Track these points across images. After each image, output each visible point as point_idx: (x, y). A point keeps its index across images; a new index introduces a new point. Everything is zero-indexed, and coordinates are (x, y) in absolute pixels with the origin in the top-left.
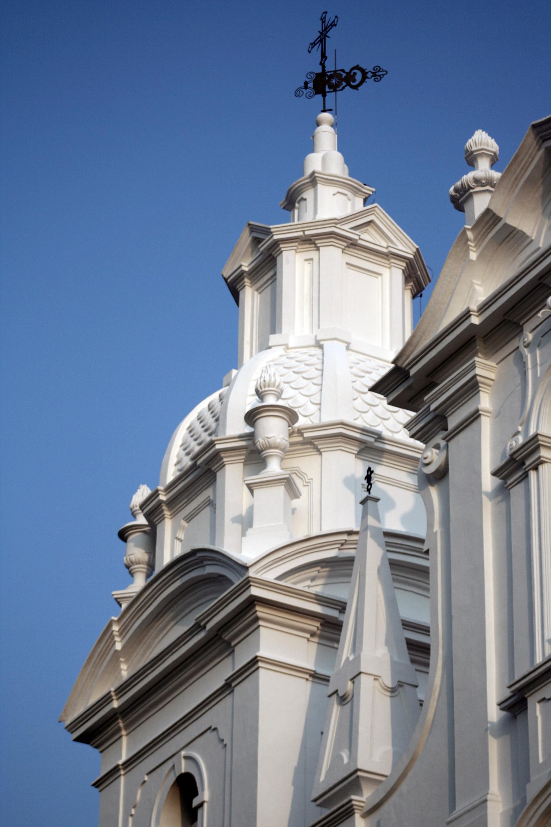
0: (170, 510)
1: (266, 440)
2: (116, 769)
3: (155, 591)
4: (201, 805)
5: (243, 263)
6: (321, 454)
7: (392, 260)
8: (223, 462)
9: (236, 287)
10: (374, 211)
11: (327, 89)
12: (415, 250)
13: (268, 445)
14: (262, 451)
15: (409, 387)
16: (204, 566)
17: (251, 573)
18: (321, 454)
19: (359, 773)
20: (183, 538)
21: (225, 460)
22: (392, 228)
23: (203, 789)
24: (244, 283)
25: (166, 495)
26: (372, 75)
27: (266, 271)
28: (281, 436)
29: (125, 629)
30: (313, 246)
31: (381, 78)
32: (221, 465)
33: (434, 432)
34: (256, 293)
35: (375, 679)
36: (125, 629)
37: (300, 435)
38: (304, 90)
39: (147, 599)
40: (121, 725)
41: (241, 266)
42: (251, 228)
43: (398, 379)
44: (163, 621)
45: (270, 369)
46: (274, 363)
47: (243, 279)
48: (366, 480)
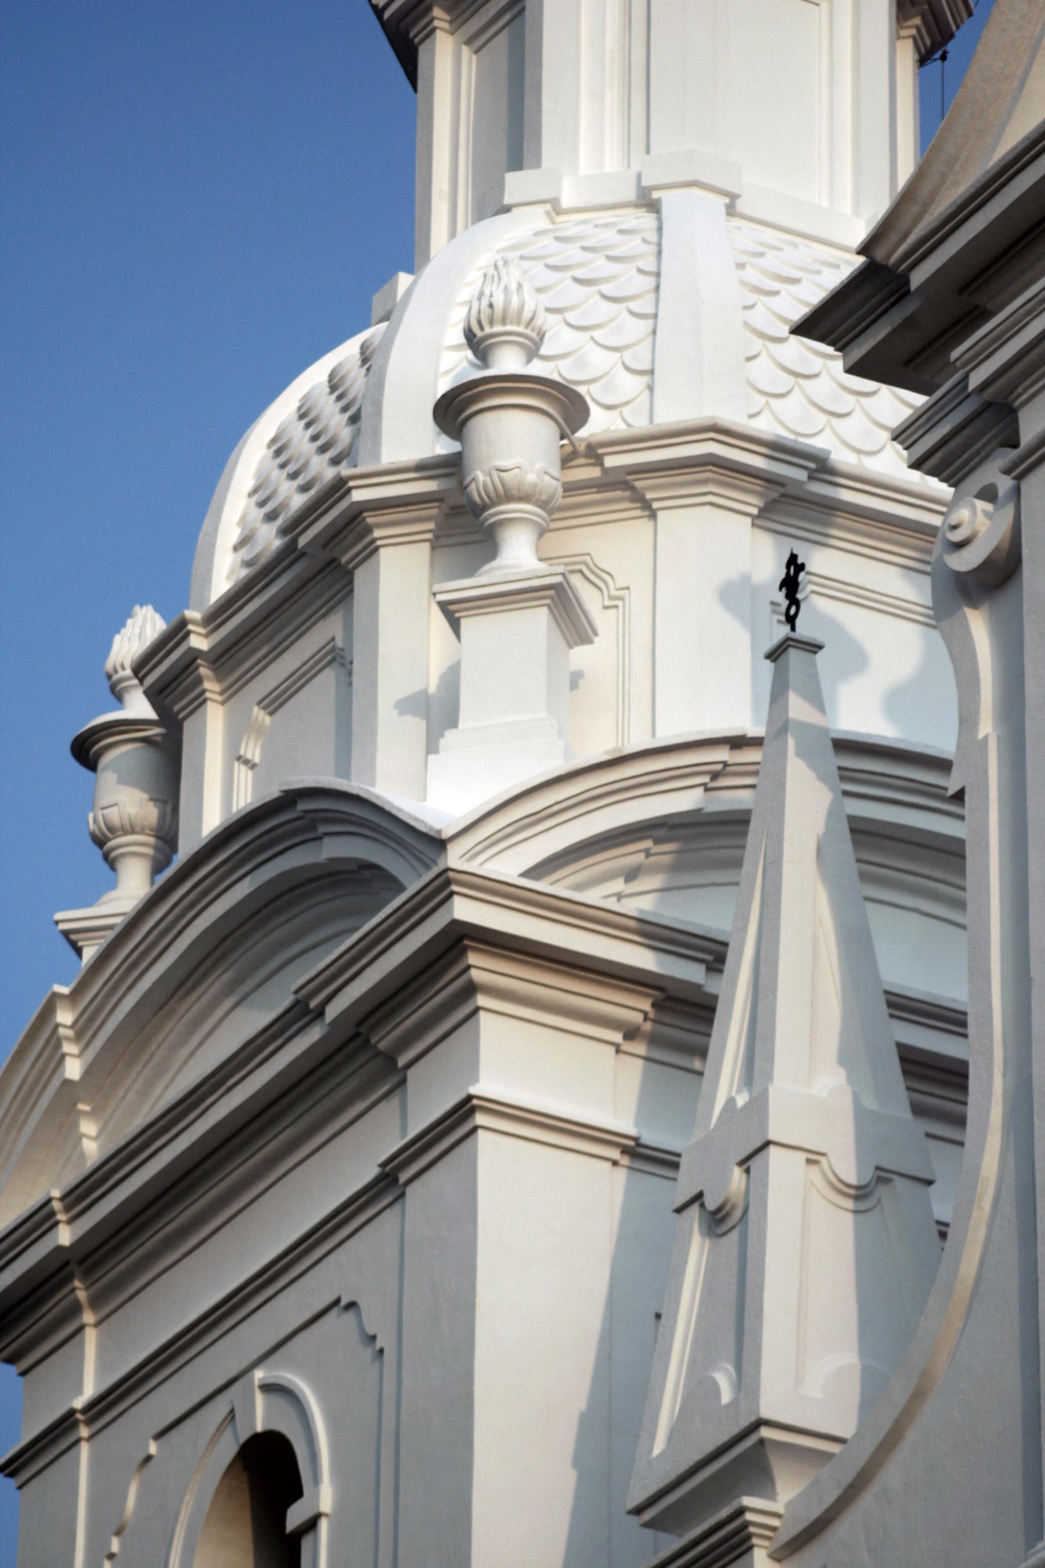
0: (219, 678)
1: (495, 474)
2: (66, 1423)
4: (311, 1525)
6: (653, 515)
8: (374, 541)
9: (408, 33)
13: (501, 491)
14: (485, 507)
15: (909, 323)
16: (319, 838)
17: (455, 858)
18: (653, 515)
19: (765, 1432)
20: (257, 760)
21: (377, 533)
23: (317, 1480)
25: (206, 636)
28: (539, 465)
29: (92, 1019)
33: (978, 452)
34: (465, 50)
35: (809, 1161)
36: (92, 1019)
37: (592, 461)
40: (82, 1295)
43: (879, 297)
44: (199, 998)
45: (507, 273)
46: (518, 253)
48: (784, 590)
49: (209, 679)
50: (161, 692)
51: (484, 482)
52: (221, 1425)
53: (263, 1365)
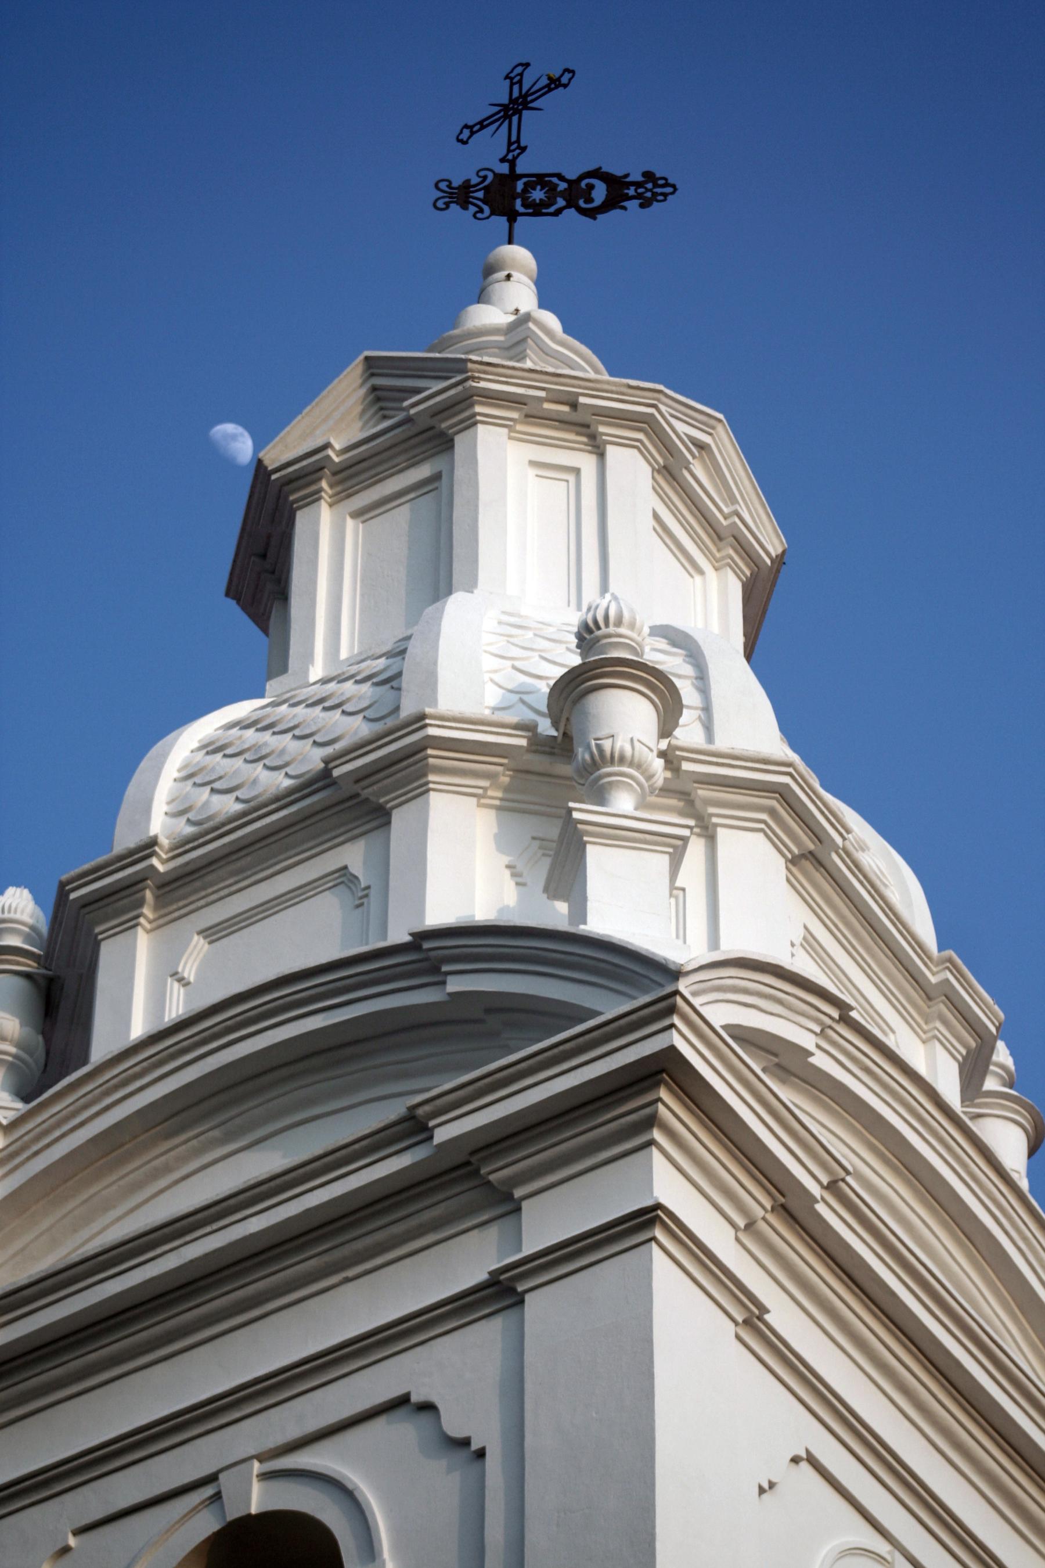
0: (156, 907)
8: (428, 783)
10: (713, 428)
50: (85, 906)
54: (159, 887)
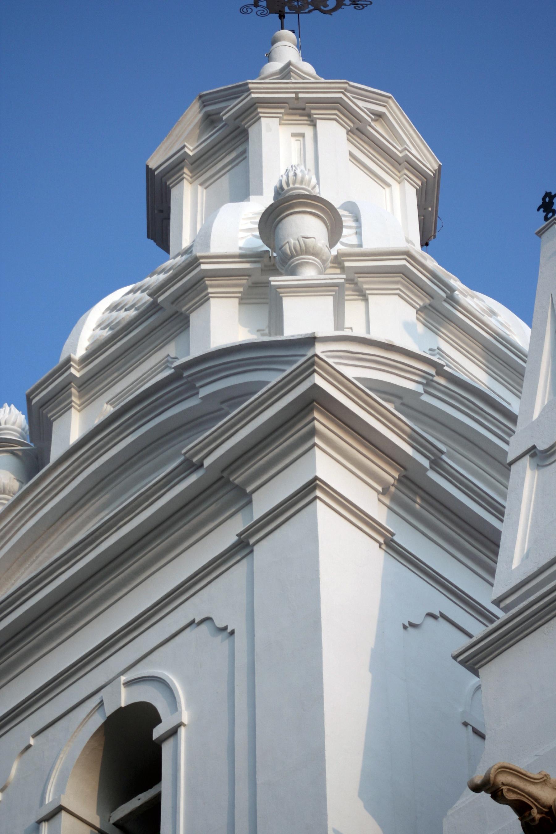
0: (80, 397)
1: (301, 240)
3: (76, 464)
4: (173, 732)
5: (186, 144)
6: (364, 297)
7: (406, 172)
10: (387, 102)
11: (287, 10)
12: (436, 167)
14: (293, 256)
18: (364, 297)
21: (210, 290)
22: (408, 131)
24: (182, 175)
25: (79, 371)
26: (351, 2)
27: (224, 154)
28: (323, 241)
30: (306, 118)
31: (364, 7)
32: (205, 296)
34: (200, 188)
37: (336, 265)
38: (253, 8)
39: (58, 479)
41: (184, 146)
42: (203, 102)
47: (182, 168)
49: (75, 397)
51: (294, 244)
52: (94, 709)
53: (125, 675)
54: (79, 387)
